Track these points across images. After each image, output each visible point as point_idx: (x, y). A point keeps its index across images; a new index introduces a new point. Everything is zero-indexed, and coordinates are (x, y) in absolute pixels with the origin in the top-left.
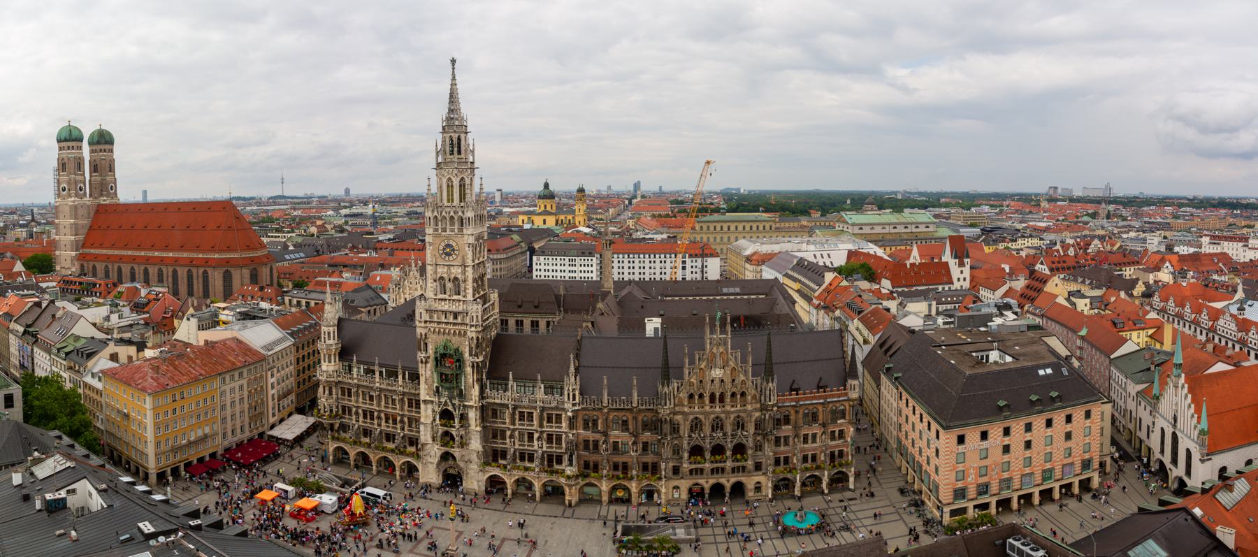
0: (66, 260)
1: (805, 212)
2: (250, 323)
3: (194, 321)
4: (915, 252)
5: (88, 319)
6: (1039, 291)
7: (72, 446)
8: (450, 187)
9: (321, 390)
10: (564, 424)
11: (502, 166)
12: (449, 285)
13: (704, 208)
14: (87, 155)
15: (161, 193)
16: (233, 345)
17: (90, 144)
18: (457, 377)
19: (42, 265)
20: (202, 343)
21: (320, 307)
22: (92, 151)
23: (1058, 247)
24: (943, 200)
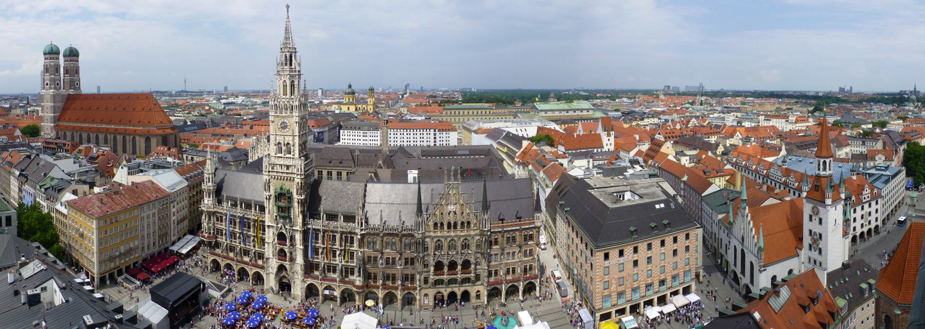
0: (48, 129)
1: (512, 103)
2: (160, 171)
3: (126, 169)
4: (580, 127)
5: (65, 166)
6: (657, 151)
7: (46, 254)
8: (285, 86)
9: (203, 217)
10: (356, 244)
11: (322, 74)
12: (284, 148)
13: (446, 101)
14: (63, 63)
15: (107, 88)
16: (150, 185)
17: (64, 56)
18: (289, 209)
19: (33, 132)
20: (130, 184)
21: (203, 163)
22: (65, 61)
23: (670, 123)
24: (598, 95)
